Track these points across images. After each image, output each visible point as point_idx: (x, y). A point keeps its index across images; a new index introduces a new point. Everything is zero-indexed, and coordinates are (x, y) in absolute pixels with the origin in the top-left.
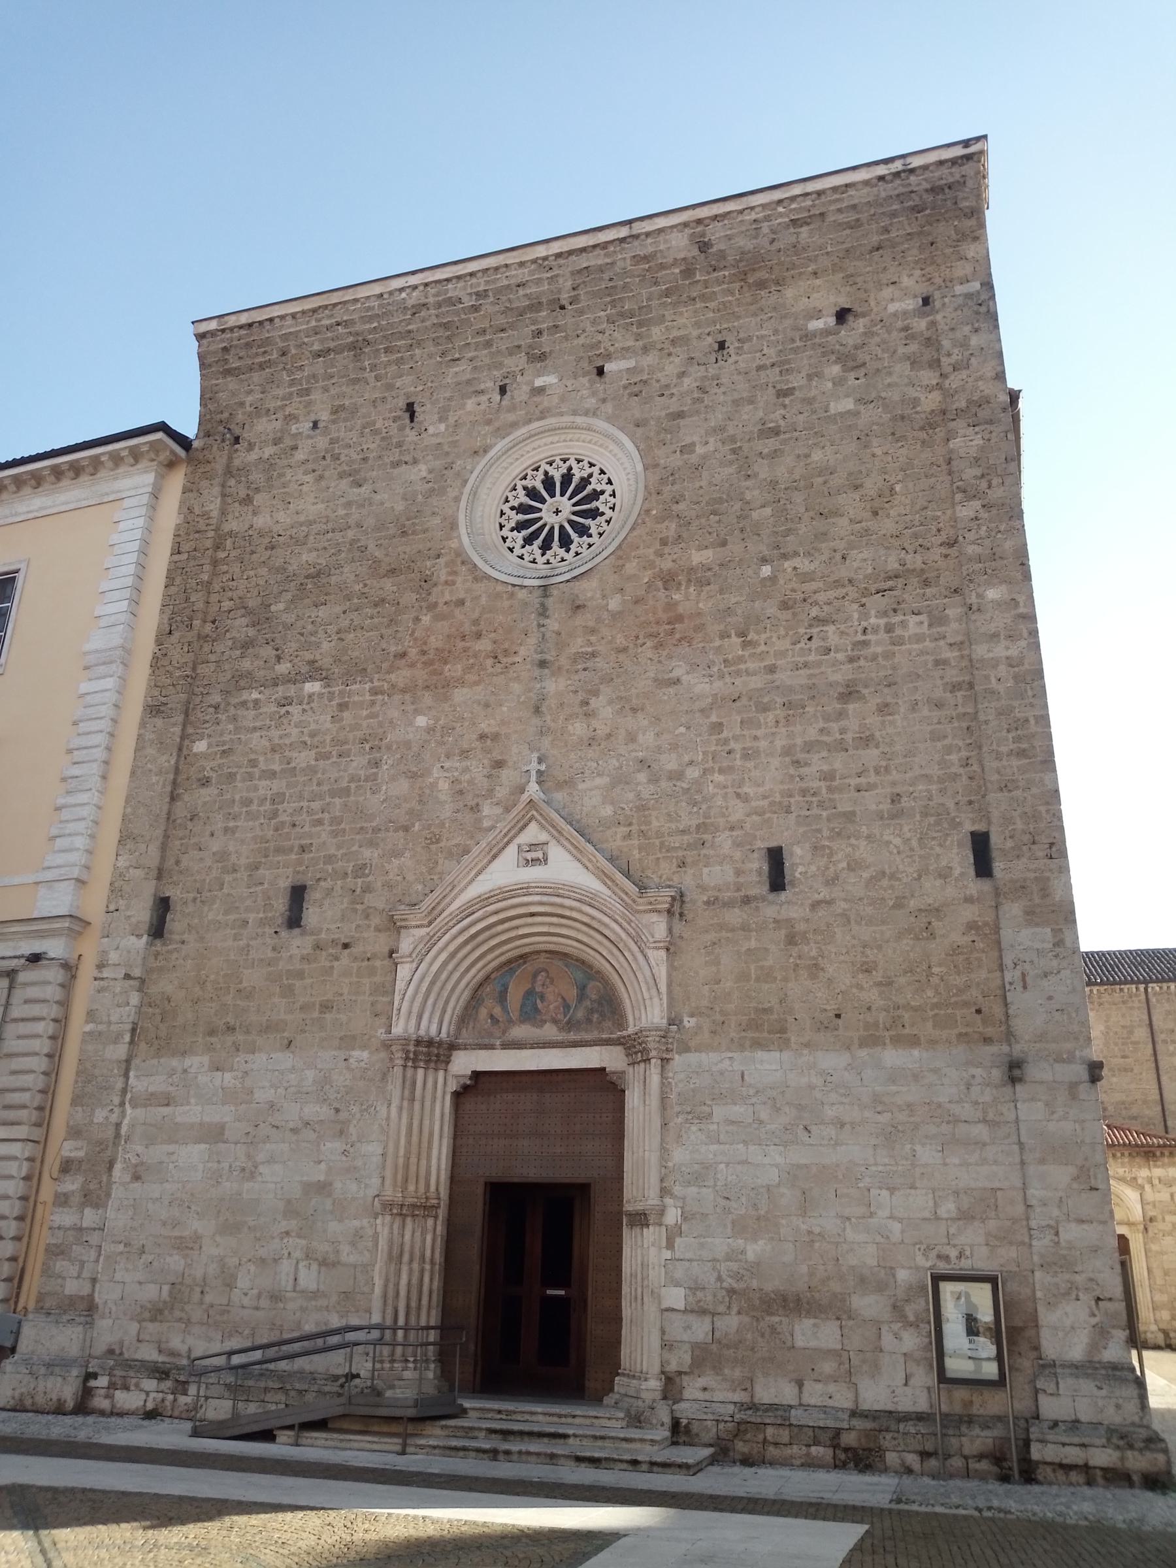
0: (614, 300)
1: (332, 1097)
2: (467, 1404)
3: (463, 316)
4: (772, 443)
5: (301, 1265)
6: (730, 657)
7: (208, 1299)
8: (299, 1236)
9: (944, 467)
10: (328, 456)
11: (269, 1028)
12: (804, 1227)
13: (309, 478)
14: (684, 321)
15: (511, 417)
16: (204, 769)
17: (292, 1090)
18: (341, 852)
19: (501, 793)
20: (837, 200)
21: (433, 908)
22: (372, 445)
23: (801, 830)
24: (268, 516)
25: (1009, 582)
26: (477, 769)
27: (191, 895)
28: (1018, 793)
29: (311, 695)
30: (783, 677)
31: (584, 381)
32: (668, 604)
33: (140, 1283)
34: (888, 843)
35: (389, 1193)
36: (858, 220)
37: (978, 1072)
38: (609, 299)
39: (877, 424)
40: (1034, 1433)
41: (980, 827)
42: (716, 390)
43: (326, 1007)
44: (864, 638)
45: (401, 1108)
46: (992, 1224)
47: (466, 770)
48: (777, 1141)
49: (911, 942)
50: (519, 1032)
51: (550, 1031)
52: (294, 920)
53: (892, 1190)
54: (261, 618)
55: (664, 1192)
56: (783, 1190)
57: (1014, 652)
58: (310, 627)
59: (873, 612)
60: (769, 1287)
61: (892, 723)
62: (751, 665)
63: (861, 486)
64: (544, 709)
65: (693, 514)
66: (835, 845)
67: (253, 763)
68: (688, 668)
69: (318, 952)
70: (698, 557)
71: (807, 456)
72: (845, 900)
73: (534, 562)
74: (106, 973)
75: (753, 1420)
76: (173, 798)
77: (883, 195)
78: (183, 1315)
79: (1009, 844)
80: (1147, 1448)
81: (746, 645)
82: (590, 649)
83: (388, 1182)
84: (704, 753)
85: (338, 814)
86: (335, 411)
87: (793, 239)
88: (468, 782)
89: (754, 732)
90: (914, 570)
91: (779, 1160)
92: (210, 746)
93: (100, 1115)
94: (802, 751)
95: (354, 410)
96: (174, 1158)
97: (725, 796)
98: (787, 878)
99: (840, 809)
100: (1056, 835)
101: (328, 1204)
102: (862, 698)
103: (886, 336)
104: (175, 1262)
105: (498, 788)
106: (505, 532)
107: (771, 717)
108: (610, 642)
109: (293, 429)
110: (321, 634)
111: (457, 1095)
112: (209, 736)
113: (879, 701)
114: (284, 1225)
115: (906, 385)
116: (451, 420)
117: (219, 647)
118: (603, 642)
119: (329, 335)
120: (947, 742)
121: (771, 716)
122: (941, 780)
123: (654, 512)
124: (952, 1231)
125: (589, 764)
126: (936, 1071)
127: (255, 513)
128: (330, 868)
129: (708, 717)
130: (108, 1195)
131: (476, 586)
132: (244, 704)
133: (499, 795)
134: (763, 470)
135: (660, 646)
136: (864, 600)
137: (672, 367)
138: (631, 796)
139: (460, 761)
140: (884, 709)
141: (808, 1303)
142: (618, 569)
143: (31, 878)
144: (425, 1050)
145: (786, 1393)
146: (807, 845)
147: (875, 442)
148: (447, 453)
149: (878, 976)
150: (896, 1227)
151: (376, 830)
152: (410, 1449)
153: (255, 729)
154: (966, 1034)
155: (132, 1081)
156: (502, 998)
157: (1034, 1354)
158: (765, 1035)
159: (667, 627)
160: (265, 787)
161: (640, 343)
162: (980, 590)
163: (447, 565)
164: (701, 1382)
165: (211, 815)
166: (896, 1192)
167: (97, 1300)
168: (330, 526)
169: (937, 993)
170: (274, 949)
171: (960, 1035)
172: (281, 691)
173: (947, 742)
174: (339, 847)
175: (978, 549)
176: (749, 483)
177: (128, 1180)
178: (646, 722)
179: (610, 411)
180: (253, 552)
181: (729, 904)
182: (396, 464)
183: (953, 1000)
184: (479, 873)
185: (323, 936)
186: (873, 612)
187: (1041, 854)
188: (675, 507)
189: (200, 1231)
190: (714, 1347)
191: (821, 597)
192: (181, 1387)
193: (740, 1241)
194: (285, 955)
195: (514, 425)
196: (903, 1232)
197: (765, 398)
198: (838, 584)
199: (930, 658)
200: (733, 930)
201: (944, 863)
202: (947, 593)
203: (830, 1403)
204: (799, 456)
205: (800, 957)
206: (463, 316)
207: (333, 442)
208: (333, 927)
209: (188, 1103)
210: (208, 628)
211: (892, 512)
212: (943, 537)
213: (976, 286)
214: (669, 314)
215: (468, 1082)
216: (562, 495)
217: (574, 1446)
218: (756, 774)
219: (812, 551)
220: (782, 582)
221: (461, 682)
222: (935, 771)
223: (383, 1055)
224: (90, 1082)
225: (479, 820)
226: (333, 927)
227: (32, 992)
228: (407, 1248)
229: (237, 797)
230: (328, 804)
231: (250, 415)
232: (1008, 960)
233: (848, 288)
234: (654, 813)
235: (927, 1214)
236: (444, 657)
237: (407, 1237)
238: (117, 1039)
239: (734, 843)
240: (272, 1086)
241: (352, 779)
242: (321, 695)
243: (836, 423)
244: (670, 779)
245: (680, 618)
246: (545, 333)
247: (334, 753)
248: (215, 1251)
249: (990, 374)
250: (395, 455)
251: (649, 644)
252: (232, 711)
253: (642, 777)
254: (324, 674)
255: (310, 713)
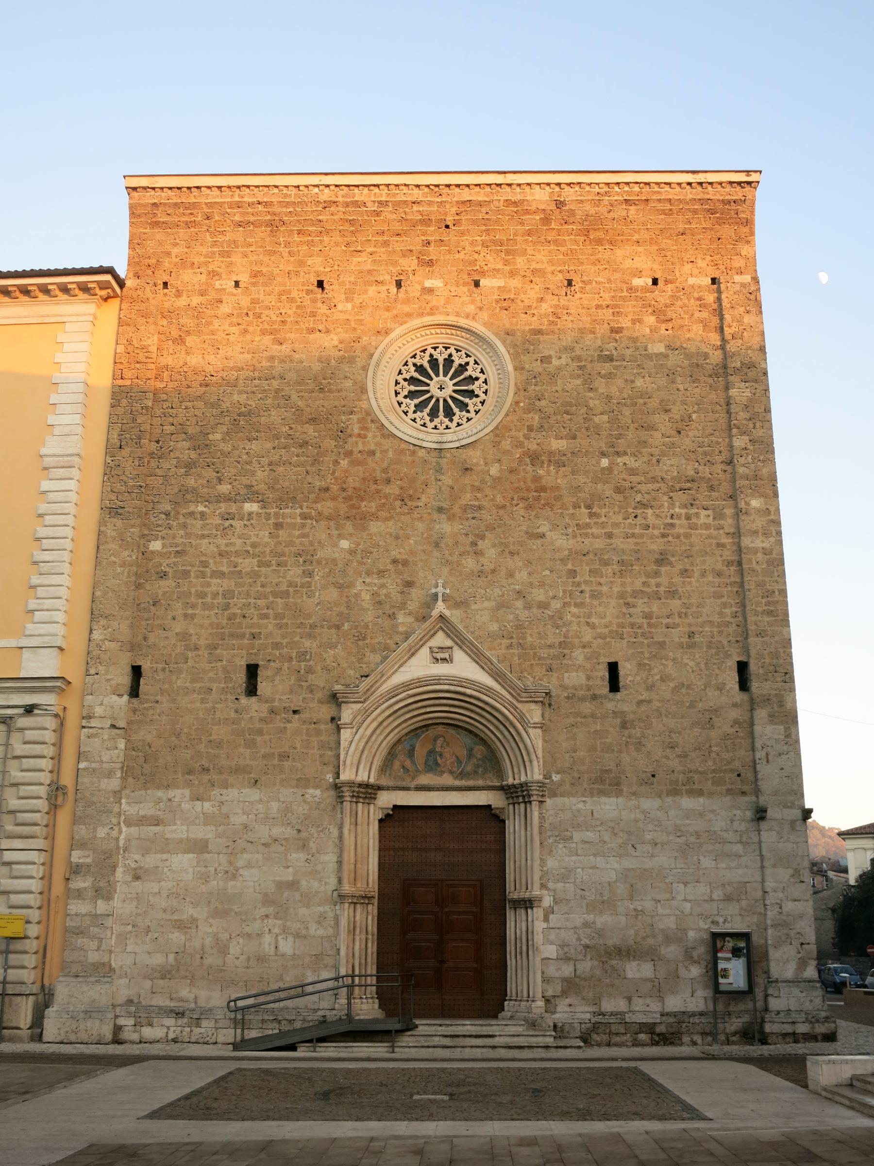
0: (488, 230)
1: (294, 822)
2: (417, 1022)
3: (366, 217)
4: (606, 368)
5: (280, 938)
6: (581, 523)
7: (208, 961)
8: (276, 918)
9: (725, 407)
10: (251, 313)
11: (239, 770)
12: (632, 907)
13: (235, 329)
14: (541, 257)
15: (406, 309)
16: (161, 565)
17: (262, 816)
18: (285, 640)
19: (412, 606)
20: (659, 192)
21: (368, 690)
22: (290, 310)
23: (630, 652)
24: (200, 357)
25: (764, 496)
26: (392, 586)
27: (160, 666)
28: (766, 639)
29: (250, 514)
30: (618, 542)
31: (466, 289)
32: (534, 476)
33: (149, 953)
34: (686, 664)
35: (347, 888)
36: (671, 210)
37: (738, 812)
38: (484, 228)
39: (680, 367)
40: (767, 1017)
41: (743, 658)
42: (565, 317)
43: (284, 756)
44: (671, 521)
45: (350, 830)
46: (744, 903)
47: (383, 586)
48: (614, 854)
49: (700, 730)
50: (425, 779)
51: (447, 780)
52: (252, 690)
53: (685, 884)
54: (201, 443)
55: (543, 886)
56: (618, 884)
57: (766, 545)
58: (245, 457)
59: (677, 504)
60: (610, 943)
61: (690, 583)
62: (595, 531)
63: (669, 410)
64: (442, 545)
65: (551, 410)
66: (652, 663)
67: (205, 564)
68: (551, 527)
69: (273, 715)
70: (557, 445)
71: (633, 382)
72: (659, 701)
73: (424, 425)
74: (93, 723)
75: (603, 1021)
76: (138, 586)
77: (690, 196)
78: (188, 974)
79: (761, 671)
80: (826, 1021)
81: (592, 515)
82: (477, 503)
83: (345, 881)
84: (564, 591)
85: (280, 611)
86: (255, 275)
87: (624, 213)
88: (385, 595)
89: (598, 579)
90: (704, 478)
91: (616, 865)
92: (164, 546)
93: (102, 832)
94: (631, 596)
95: (271, 278)
96: (167, 863)
97: (579, 623)
98: (621, 684)
99: (656, 639)
100: (789, 667)
101: (297, 896)
102: (671, 564)
103: (686, 301)
104: (177, 937)
105: (409, 602)
106: (400, 398)
107: (610, 570)
108: (492, 500)
109: (217, 284)
110: (255, 464)
111: (381, 821)
112: (163, 538)
113: (681, 567)
114: (264, 911)
115: (700, 342)
116: (357, 301)
117: (165, 464)
118: (487, 499)
119: (250, 210)
120: (724, 600)
121: (610, 570)
122: (719, 626)
123: (522, 404)
124: (720, 907)
125: (479, 590)
126: (712, 811)
127: (188, 353)
128: (277, 653)
129: (566, 565)
130: (115, 891)
131: (383, 441)
132: (192, 514)
133: (410, 608)
134: (601, 385)
135: (529, 507)
136: (672, 494)
137: (533, 293)
138: (511, 617)
139: (379, 578)
140: (684, 572)
141: (634, 952)
142: (496, 444)
143: (12, 643)
144: (363, 790)
145: (621, 1005)
146: (635, 663)
147: (679, 380)
148: (355, 329)
149: (679, 751)
150: (688, 906)
151: (313, 626)
152: (396, 1050)
153: (203, 536)
154: (732, 789)
155: (124, 806)
156: (411, 753)
157: (765, 976)
158: (607, 786)
159: (535, 494)
161: (508, 268)
162: (747, 499)
163: (359, 421)
164: (568, 1001)
165: (171, 602)
166: (689, 885)
167: (113, 965)
168: (257, 374)
169: (715, 763)
170: (236, 711)
171: (728, 790)
172: (223, 507)
173: (724, 600)
174: (284, 637)
175: (746, 471)
176: (591, 395)
177: (130, 879)
178: (520, 564)
179: (486, 319)
180: (189, 387)
181: (583, 699)
182: (311, 331)
183: (724, 768)
184: (401, 666)
185: (276, 704)
186: (677, 504)
187: (779, 679)
188: (537, 403)
189: (195, 916)
190: (577, 980)
191: (643, 488)
192: (197, 1022)
193: (592, 916)
194: (246, 716)
195: (409, 315)
196: (691, 908)
197: (602, 331)
198: (654, 480)
199: (714, 541)
200: (585, 717)
201: (720, 681)
202: (725, 497)
203: (648, 1009)
204: (626, 380)
205: (629, 737)
206: (366, 217)
207: (254, 301)
208: (284, 698)
209: (175, 824)
210: (153, 446)
211: (690, 433)
212: (723, 457)
213: (747, 278)
214: (530, 249)
215: (391, 812)
216: (451, 379)
217: (497, 1041)
218: (600, 609)
219: (637, 453)
220: (616, 472)
221: (375, 517)
222: (716, 619)
223: (332, 793)
224: (89, 806)
225: (396, 626)
226: (284, 698)
227: (30, 735)
228: (358, 925)
229: (193, 590)
230: (272, 603)
231: (176, 264)
232: (758, 745)
233: (660, 259)
234: (529, 632)
235: (706, 898)
236: (360, 495)
237: (358, 918)
238: (110, 774)
239: (585, 656)
240: (244, 813)
241: (290, 584)
242: (258, 514)
243: (652, 361)
244: (539, 607)
245: (543, 489)
246: (432, 244)
247: (273, 562)
248: (210, 930)
249: (756, 347)
250: (309, 323)
251: (521, 505)
252: (182, 520)
253: (519, 604)
254: (260, 498)
255: (250, 527)
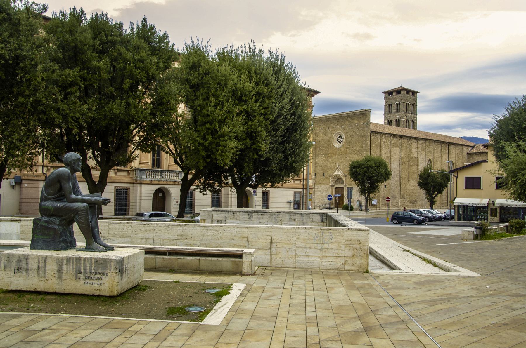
4: (353, 136)
54: (320, 149)
70: (348, 146)
160: (321, 164)
236: (332, 154)
